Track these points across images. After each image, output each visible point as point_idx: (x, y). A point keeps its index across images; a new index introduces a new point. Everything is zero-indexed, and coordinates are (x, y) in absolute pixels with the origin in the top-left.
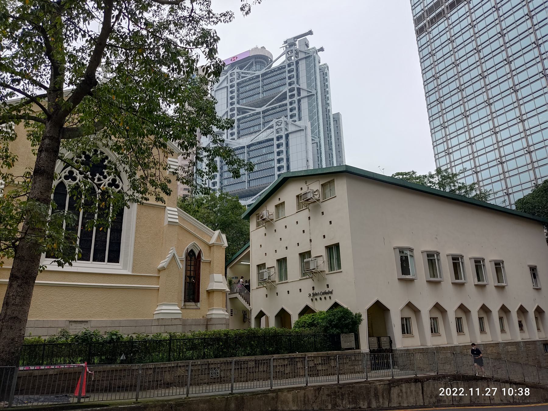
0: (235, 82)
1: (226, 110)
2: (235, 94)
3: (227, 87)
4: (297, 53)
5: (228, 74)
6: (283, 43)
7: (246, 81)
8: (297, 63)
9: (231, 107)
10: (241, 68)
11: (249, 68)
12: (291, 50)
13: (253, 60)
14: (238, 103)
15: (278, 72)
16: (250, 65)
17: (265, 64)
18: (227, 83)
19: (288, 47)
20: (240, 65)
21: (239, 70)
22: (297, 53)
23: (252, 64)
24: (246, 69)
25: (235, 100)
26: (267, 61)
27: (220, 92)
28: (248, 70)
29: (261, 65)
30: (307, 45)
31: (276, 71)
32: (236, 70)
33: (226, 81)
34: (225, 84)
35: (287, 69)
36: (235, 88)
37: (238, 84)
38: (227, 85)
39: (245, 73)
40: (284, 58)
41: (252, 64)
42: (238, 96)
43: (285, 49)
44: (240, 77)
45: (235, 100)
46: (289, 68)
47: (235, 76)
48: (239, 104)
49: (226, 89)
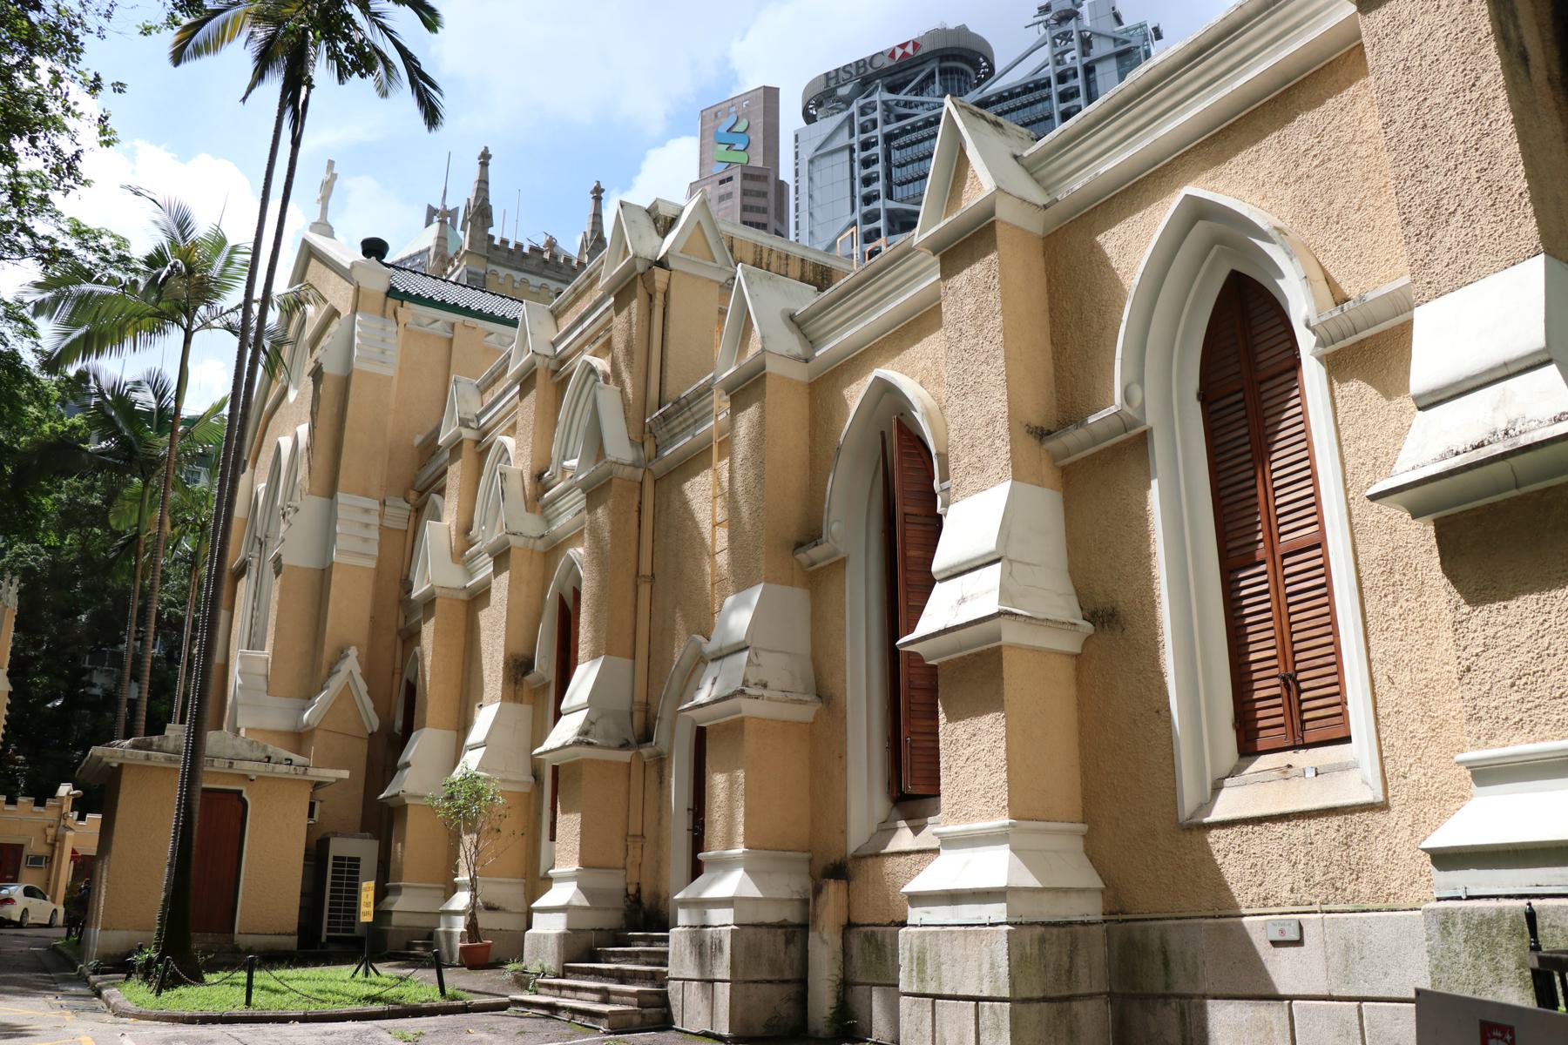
0: (878, 133)
1: (848, 219)
2: (879, 168)
3: (852, 150)
4: (1086, 43)
5: (854, 108)
6: (1037, 12)
7: (914, 128)
8: (1089, 69)
9: (866, 209)
10: (893, 89)
11: (920, 89)
12: (1065, 34)
13: (933, 65)
14: (889, 196)
15: (1024, 99)
16: (922, 81)
17: (967, 75)
18: (852, 135)
19: (1052, 22)
20: (889, 79)
21: (888, 96)
22: (1086, 43)
23: (931, 76)
24: (910, 91)
25: (879, 186)
26: (976, 66)
27: (827, 162)
28: (916, 95)
29: (959, 80)
30: (1118, 18)
31: (1018, 95)
32: (880, 96)
33: (846, 131)
34: (843, 139)
35: (1056, 88)
36: (878, 150)
37: (889, 138)
38: (851, 141)
39: (907, 104)
40: (1045, 53)
41: (931, 76)
42: (888, 176)
43: (1043, 31)
44: (892, 116)
45: (879, 186)
46: (1062, 87)
47: (878, 115)
48: (892, 199)
49: (847, 154)
